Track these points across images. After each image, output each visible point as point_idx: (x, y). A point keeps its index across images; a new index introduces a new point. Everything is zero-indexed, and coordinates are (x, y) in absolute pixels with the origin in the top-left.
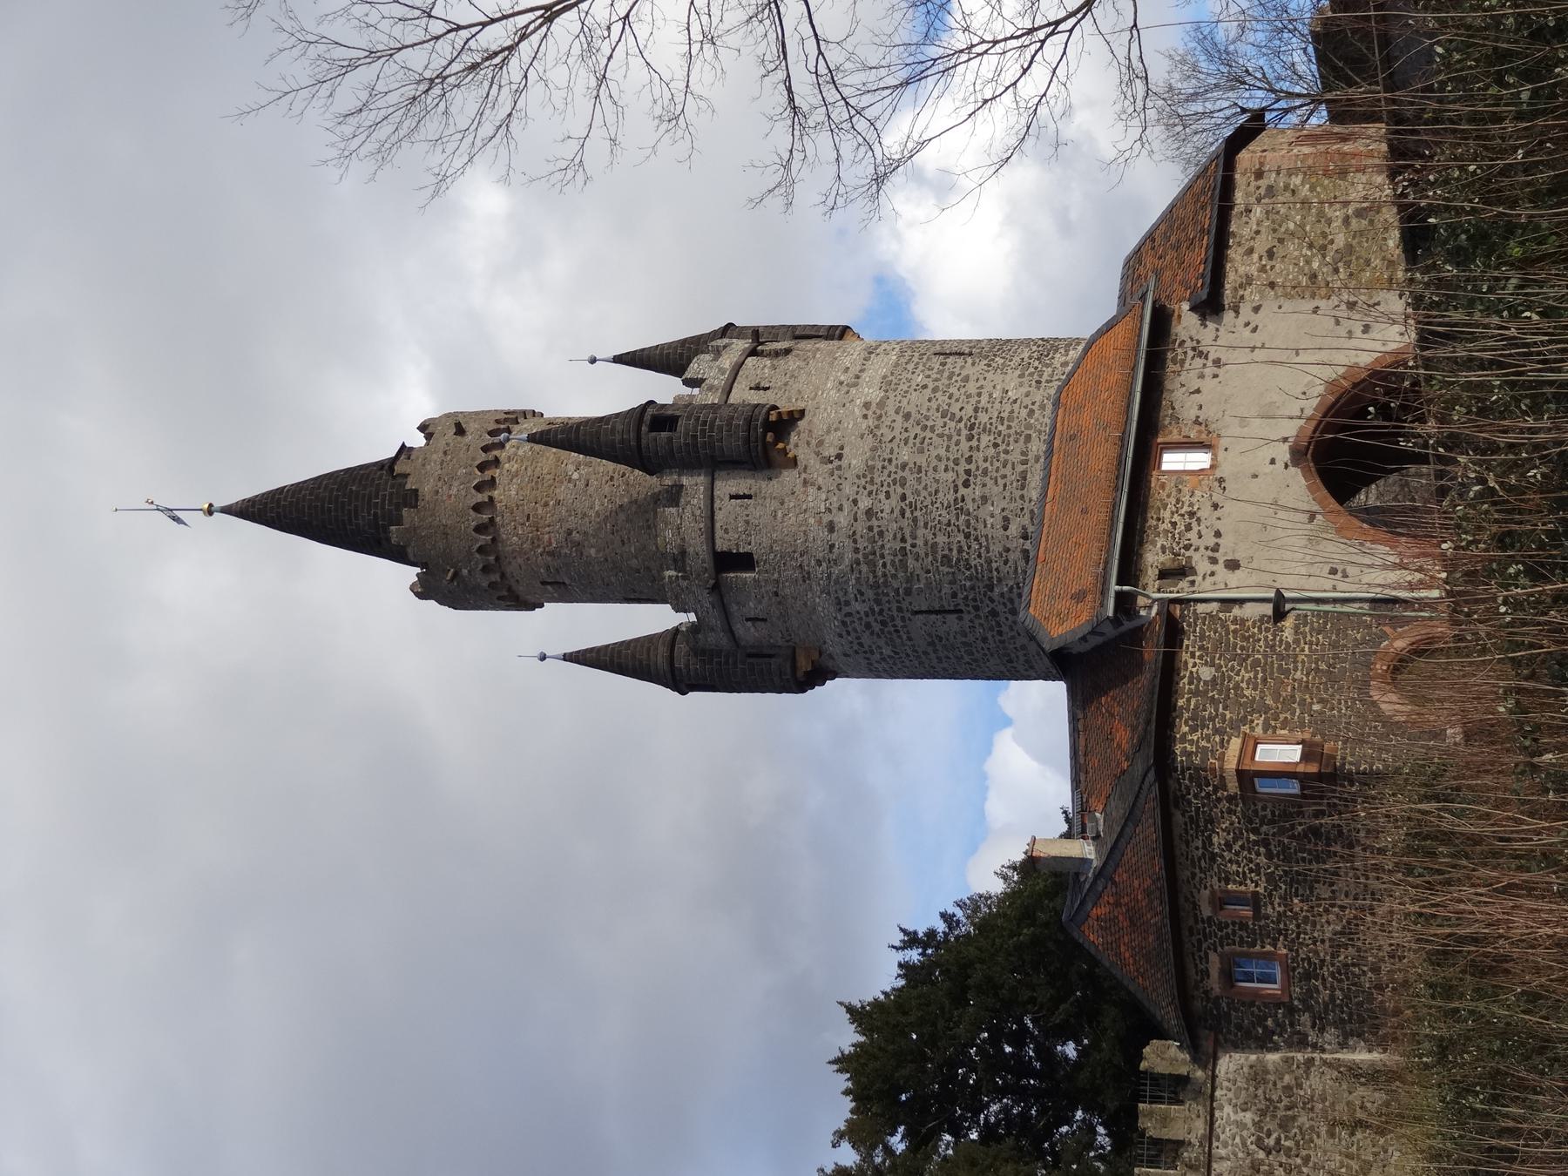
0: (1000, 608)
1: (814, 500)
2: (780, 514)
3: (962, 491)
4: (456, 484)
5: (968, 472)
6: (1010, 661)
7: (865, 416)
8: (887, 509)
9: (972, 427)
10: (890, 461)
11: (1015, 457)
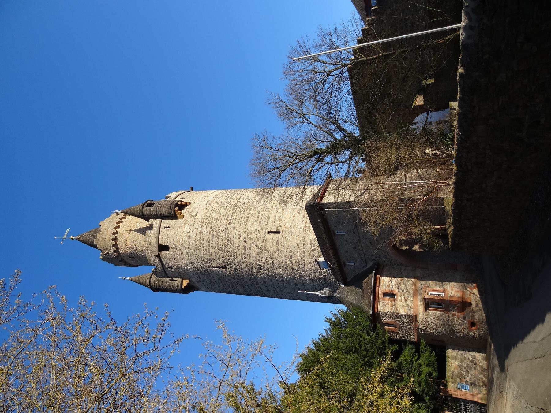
1: (186, 228)
3: (228, 226)
6: (244, 287)
11: (246, 215)
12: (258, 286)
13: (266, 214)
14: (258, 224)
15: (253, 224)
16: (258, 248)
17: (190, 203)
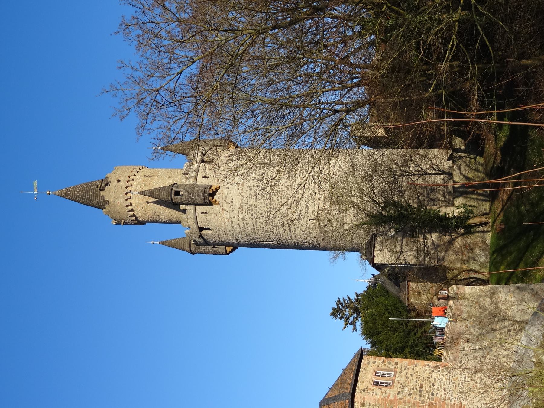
4: (120, 199)
5: (271, 208)
7: (238, 189)
17: (219, 188)
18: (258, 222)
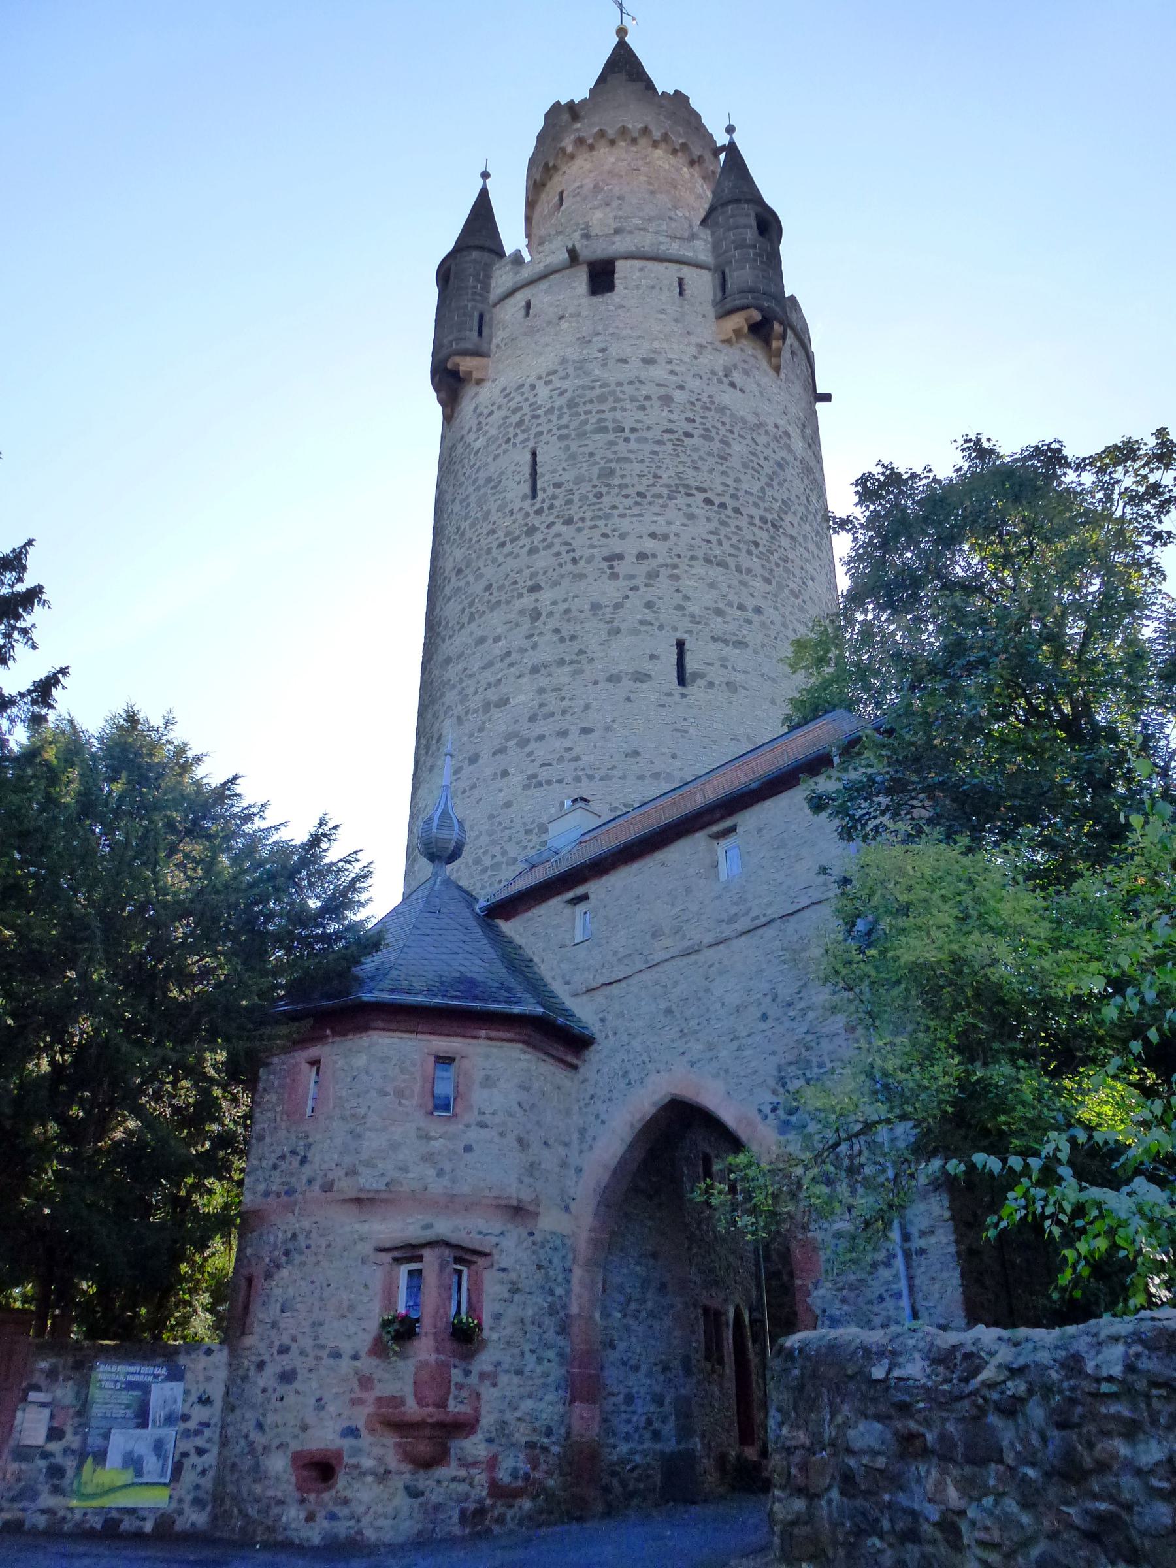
0: (538, 536)
2: (662, 316)
7: (776, 426)
8: (671, 416)
9: (773, 525)
10: (732, 432)
12: (465, 619)
13: (753, 636)
14: (712, 605)
15: (712, 585)
16: (618, 606)
18: (656, 448)
